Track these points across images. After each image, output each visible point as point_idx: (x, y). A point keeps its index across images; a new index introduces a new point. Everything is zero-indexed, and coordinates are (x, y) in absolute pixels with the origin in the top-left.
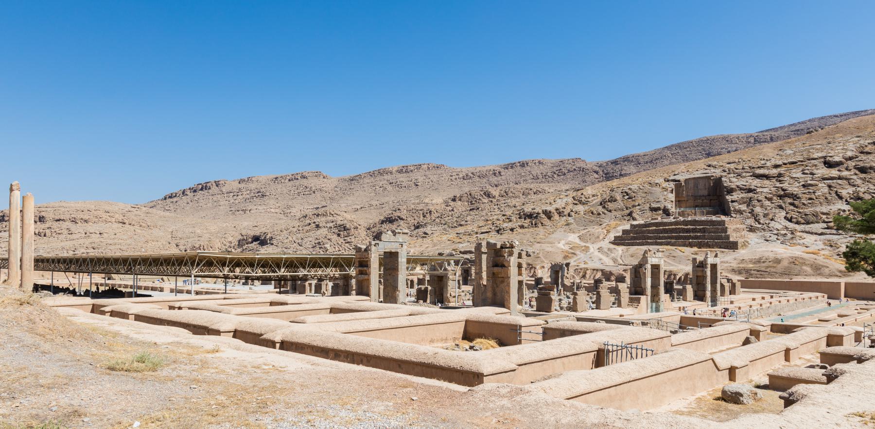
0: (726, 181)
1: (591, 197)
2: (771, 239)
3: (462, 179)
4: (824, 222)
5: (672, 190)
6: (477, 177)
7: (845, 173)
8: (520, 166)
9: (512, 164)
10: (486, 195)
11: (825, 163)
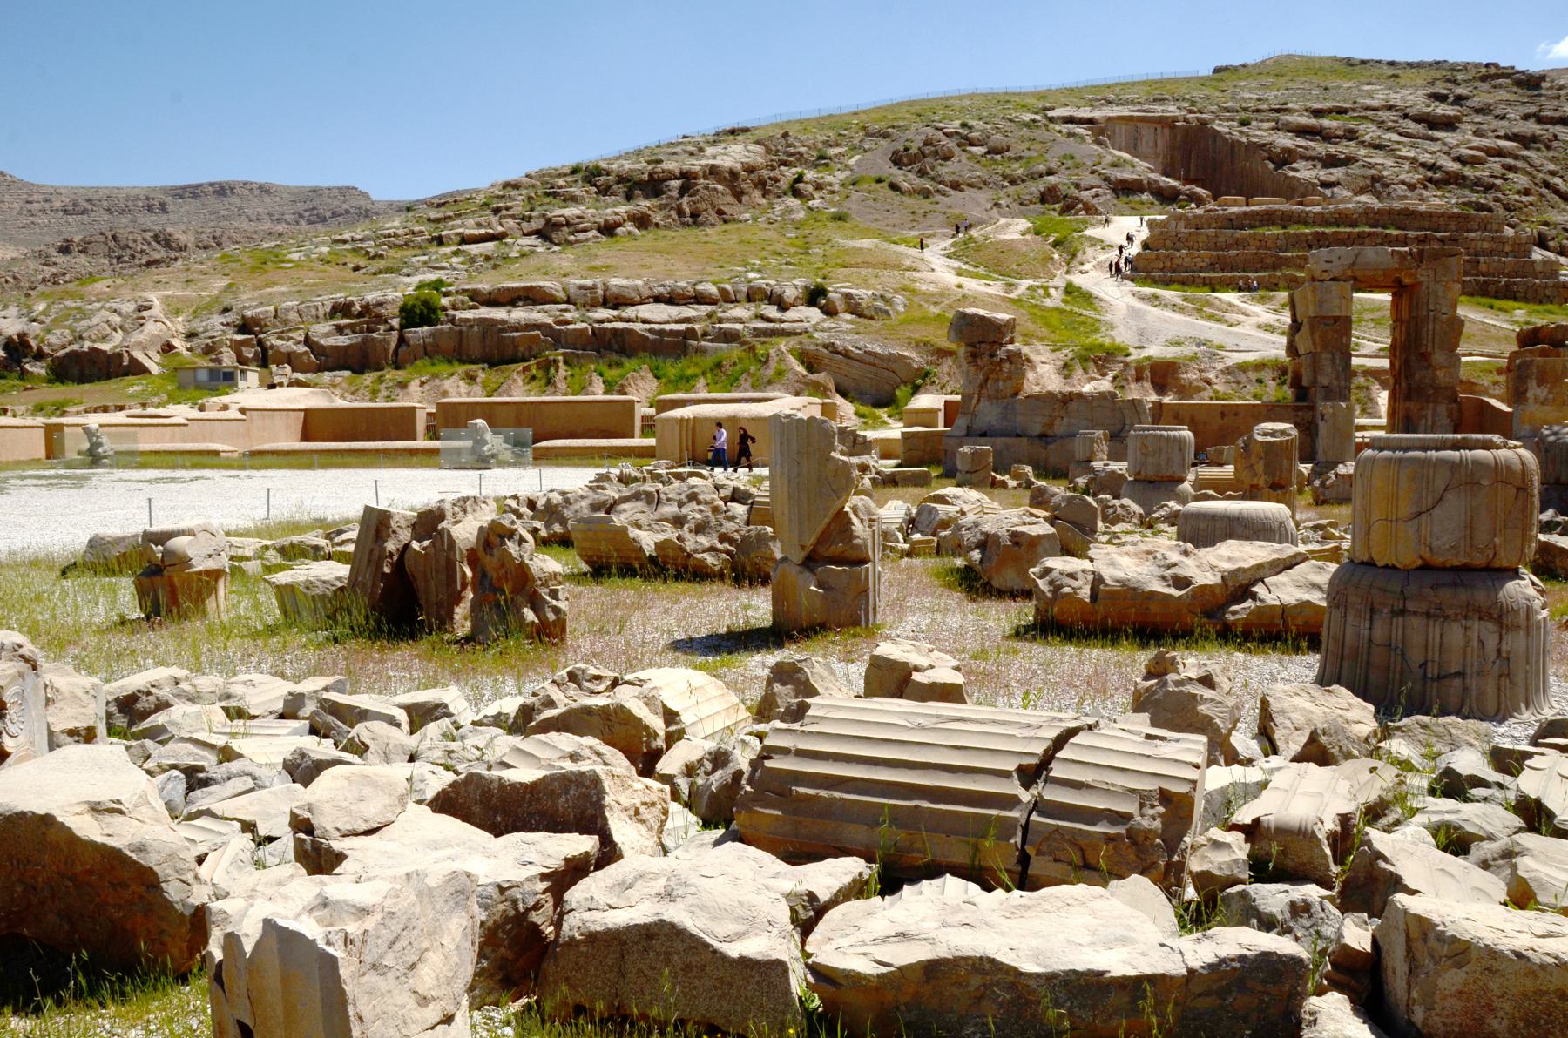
3: (61, 213)
6: (102, 211)
8: (214, 192)
10: (159, 243)
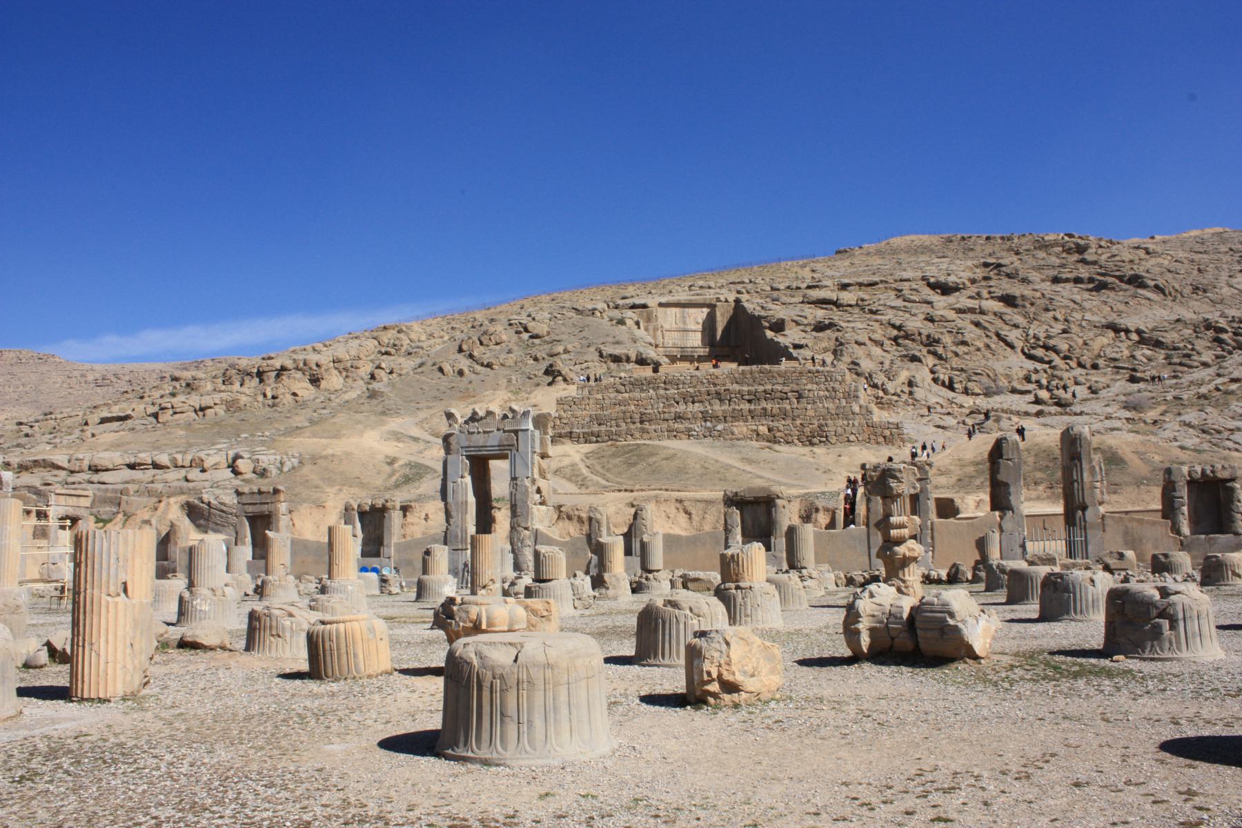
1: (423, 338)
6: (125, 383)
9: (197, 362)
11: (933, 286)
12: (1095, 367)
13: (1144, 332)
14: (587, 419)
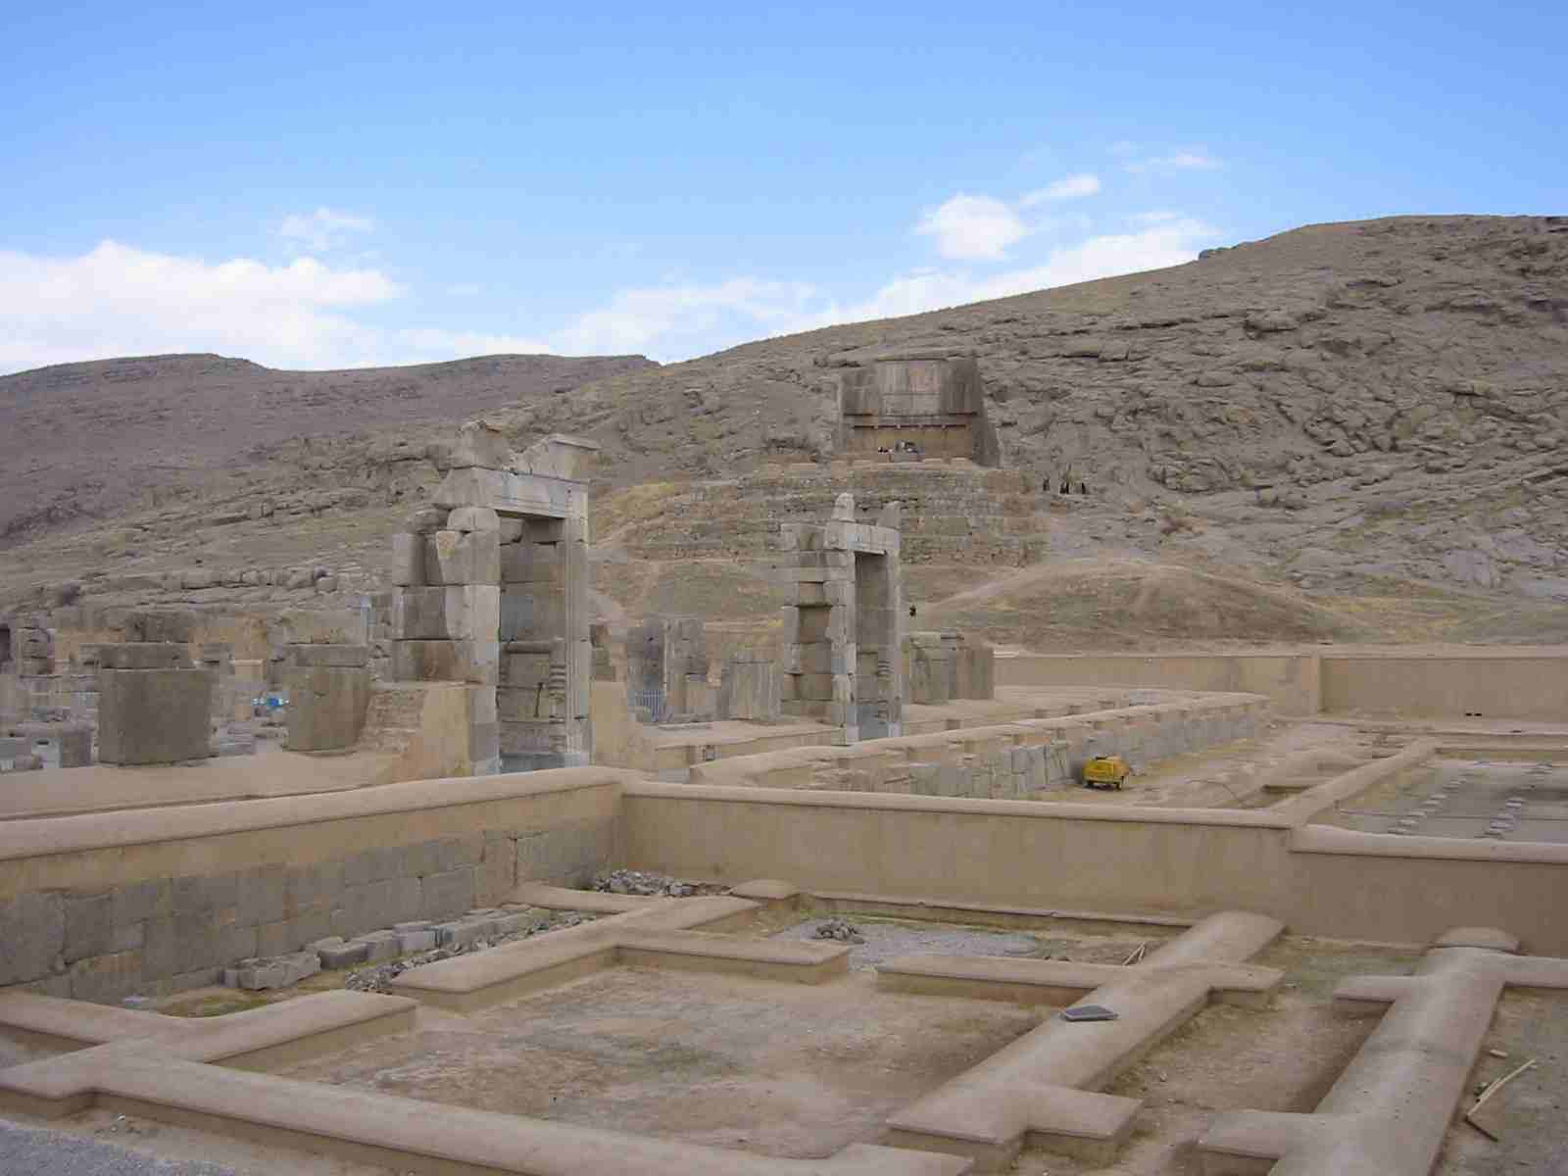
0: (987, 368)
1: (589, 410)
2: (1110, 534)
4: (1249, 487)
5: (836, 388)
7: (1299, 356)
11: (1249, 326)
12: (1394, 448)
13: (1496, 397)
14: (690, 530)
